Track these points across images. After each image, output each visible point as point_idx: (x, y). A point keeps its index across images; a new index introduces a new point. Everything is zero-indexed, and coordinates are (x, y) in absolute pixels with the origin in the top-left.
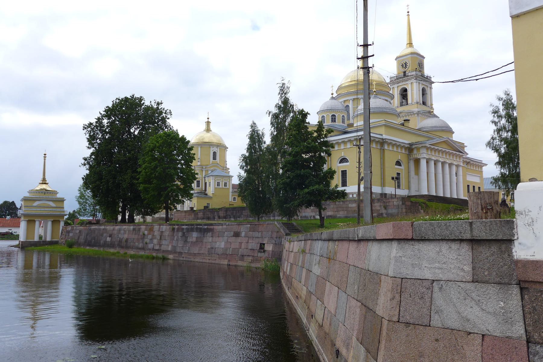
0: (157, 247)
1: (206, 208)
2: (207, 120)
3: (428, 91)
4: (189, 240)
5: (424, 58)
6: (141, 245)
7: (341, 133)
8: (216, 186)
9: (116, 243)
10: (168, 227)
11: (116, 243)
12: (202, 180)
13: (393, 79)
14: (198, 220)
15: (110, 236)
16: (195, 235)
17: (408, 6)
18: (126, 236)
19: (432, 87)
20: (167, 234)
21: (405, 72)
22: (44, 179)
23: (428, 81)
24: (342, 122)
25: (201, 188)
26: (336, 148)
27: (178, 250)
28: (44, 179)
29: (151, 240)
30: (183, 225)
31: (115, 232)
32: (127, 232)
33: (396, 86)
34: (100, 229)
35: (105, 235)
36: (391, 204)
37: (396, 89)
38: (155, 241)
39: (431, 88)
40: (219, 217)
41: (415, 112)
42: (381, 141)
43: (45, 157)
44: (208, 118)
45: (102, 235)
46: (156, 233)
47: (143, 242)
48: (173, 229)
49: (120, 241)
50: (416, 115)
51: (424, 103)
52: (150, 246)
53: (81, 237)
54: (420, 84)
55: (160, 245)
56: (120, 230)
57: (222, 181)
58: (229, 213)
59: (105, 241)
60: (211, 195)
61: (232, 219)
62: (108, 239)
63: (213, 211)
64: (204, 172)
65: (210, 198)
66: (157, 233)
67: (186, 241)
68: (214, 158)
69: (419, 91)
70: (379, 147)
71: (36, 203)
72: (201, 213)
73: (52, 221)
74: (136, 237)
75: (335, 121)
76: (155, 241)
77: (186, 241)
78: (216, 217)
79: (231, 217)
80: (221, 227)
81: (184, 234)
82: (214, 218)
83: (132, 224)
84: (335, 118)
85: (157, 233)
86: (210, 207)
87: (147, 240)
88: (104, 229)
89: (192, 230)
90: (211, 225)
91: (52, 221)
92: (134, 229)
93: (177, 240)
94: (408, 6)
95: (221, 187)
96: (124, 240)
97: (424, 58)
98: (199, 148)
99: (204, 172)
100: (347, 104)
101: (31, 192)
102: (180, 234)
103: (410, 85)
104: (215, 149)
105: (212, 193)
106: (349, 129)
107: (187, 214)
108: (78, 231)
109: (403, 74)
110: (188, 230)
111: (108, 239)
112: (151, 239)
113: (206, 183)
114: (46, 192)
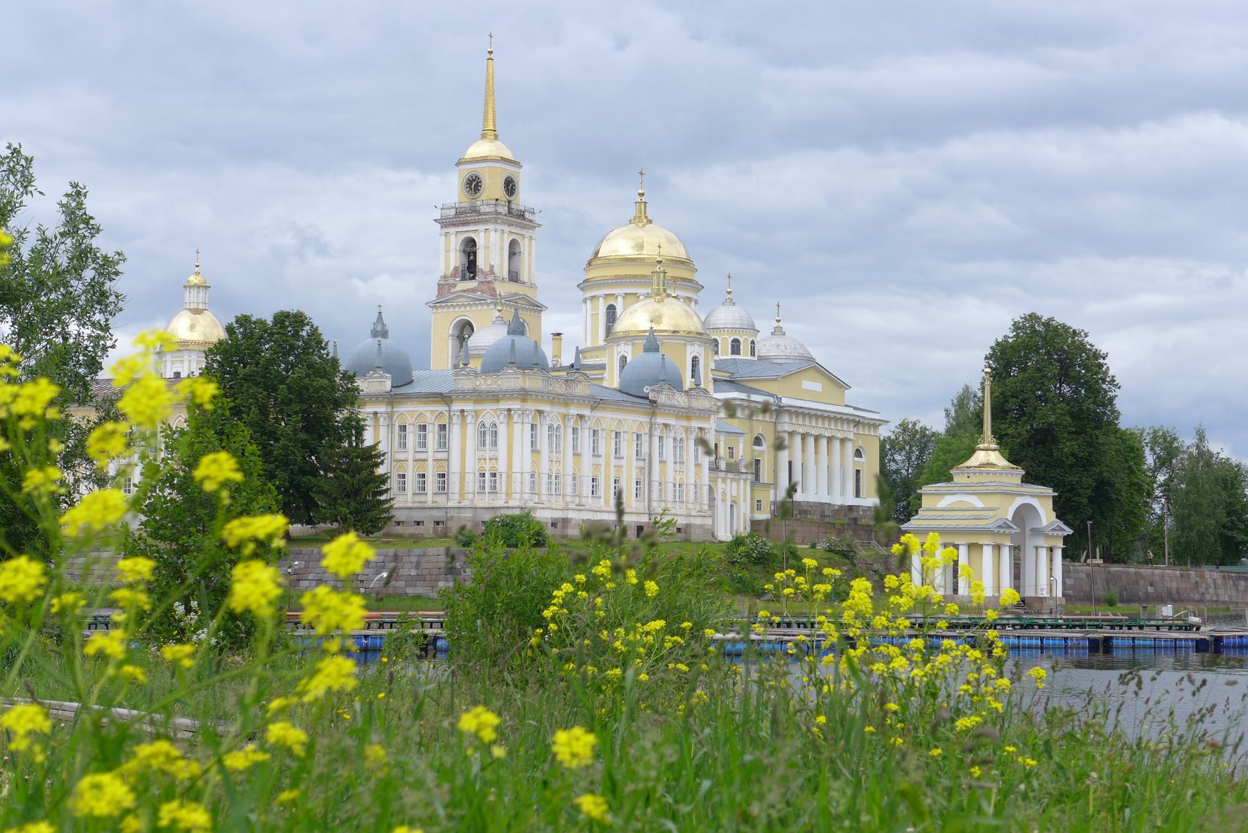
0: (1215, 598)
4: (1240, 588)
6: (1197, 597)
9: (1165, 595)
11: (1165, 595)
15: (1151, 585)
18: (1174, 585)
20: (1219, 581)
27: (1234, 600)
29: (1207, 589)
31: (1157, 579)
34: (1128, 574)
38: (1211, 591)
45: (1137, 583)
48: (1224, 577)
49: (1169, 592)
52: (1208, 597)
55: (1218, 596)
56: (1162, 577)
59: (1147, 593)
62: (1150, 589)
66: (1210, 581)
67: (1237, 590)
69: (502, 248)
75: (738, 353)
76: (1211, 591)
77: (1237, 590)
83: (1178, 568)
84: (738, 347)
85: (1210, 581)
87: (1202, 590)
88: (1136, 573)
96: (1174, 591)
102: (1231, 582)
108: (1083, 576)
111: (1150, 589)
112: (1207, 589)
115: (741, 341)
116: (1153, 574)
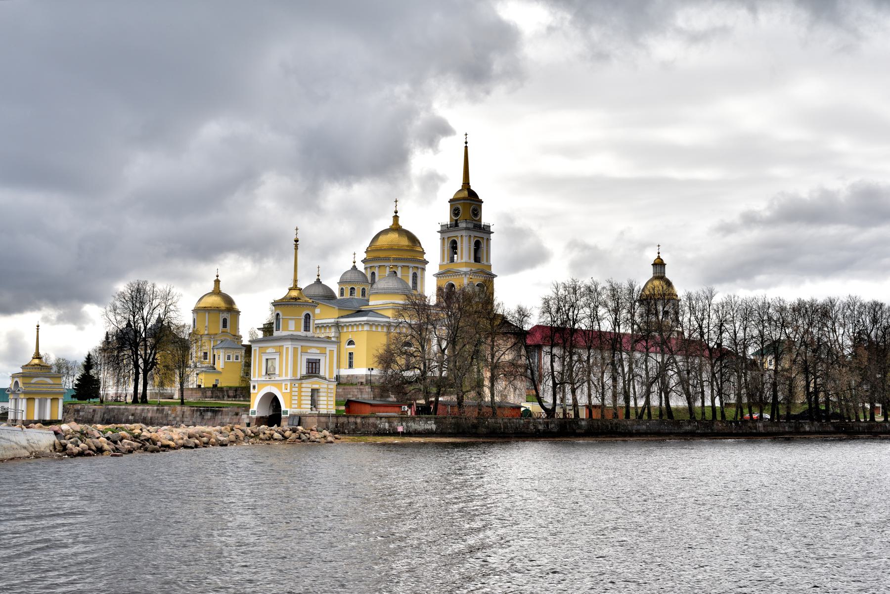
1: (215, 386)
2: (216, 278)
3: (483, 245)
4: (206, 417)
5: (483, 202)
7: (354, 312)
8: (226, 360)
10: (189, 408)
12: (210, 352)
13: (445, 228)
14: (206, 399)
15: (133, 415)
16: (209, 414)
17: (466, 135)
18: (150, 415)
19: (491, 238)
21: (456, 221)
22: (37, 353)
23: (487, 230)
24: (362, 295)
25: (210, 361)
26: (345, 330)
28: (37, 353)
30: (201, 407)
31: (138, 412)
32: (151, 412)
33: (446, 235)
34: (120, 409)
35: (126, 414)
36: (364, 390)
37: (446, 240)
39: (488, 240)
40: (229, 397)
41: (462, 273)
42: (387, 324)
43: (38, 329)
44: (217, 276)
45: (123, 414)
46: (178, 413)
47: (167, 420)
50: (463, 276)
51: (477, 259)
53: (96, 416)
54: (472, 238)
56: (143, 410)
57: (233, 354)
58: (238, 392)
60: (220, 370)
61: (242, 399)
62: (130, 417)
63: (221, 389)
64: (212, 342)
65: (219, 373)
67: (203, 418)
68: (225, 326)
70: (385, 330)
71: (34, 380)
72: (210, 392)
73: (51, 399)
74: (160, 415)
77: (203, 418)
78: (226, 398)
79: (240, 397)
80: (227, 409)
81: (201, 414)
82: (223, 397)
86: (219, 385)
88: (124, 409)
89: (207, 411)
90: (221, 407)
91: (51, 399)
92: (158, 410)
93: (196, 417)
94: (466, 135)
95: (231, 360)
97: (483, 202)
98: (207, 314)
99: (212, 342)
100: (373, 270)
101: (23, 367)
102: (199, 413)
103: (460, 238)
104: (225, 315)
105: (221, 367)
106: (364, 308)
107: (194, 392)
108: (92, 410)
109: (454, 222)
110: (204, 411)
111: (130, 417)
112: (175, 418)
113: (214, 356)
114: (43, 367)
115: (356, 288)
116: (136, 409)
